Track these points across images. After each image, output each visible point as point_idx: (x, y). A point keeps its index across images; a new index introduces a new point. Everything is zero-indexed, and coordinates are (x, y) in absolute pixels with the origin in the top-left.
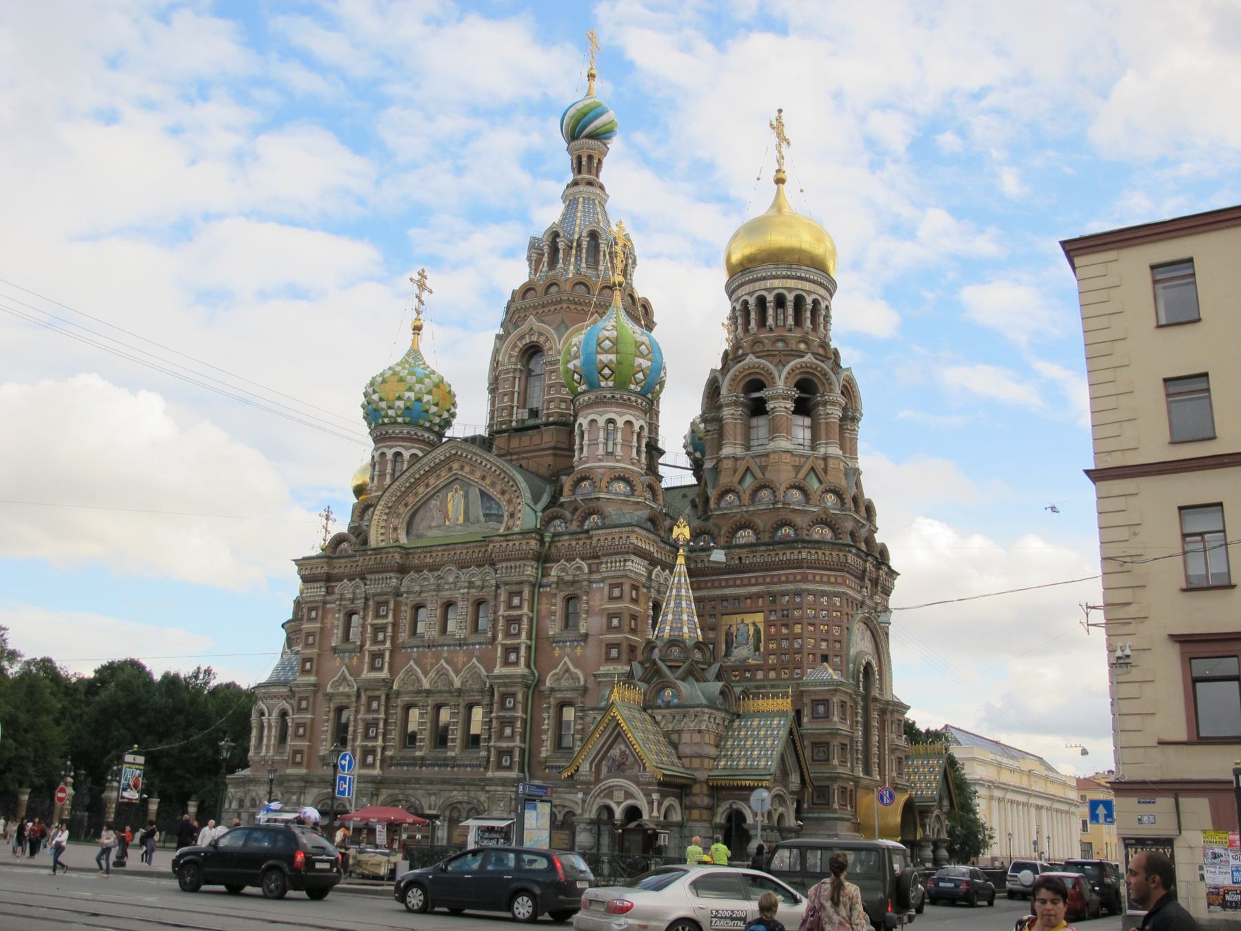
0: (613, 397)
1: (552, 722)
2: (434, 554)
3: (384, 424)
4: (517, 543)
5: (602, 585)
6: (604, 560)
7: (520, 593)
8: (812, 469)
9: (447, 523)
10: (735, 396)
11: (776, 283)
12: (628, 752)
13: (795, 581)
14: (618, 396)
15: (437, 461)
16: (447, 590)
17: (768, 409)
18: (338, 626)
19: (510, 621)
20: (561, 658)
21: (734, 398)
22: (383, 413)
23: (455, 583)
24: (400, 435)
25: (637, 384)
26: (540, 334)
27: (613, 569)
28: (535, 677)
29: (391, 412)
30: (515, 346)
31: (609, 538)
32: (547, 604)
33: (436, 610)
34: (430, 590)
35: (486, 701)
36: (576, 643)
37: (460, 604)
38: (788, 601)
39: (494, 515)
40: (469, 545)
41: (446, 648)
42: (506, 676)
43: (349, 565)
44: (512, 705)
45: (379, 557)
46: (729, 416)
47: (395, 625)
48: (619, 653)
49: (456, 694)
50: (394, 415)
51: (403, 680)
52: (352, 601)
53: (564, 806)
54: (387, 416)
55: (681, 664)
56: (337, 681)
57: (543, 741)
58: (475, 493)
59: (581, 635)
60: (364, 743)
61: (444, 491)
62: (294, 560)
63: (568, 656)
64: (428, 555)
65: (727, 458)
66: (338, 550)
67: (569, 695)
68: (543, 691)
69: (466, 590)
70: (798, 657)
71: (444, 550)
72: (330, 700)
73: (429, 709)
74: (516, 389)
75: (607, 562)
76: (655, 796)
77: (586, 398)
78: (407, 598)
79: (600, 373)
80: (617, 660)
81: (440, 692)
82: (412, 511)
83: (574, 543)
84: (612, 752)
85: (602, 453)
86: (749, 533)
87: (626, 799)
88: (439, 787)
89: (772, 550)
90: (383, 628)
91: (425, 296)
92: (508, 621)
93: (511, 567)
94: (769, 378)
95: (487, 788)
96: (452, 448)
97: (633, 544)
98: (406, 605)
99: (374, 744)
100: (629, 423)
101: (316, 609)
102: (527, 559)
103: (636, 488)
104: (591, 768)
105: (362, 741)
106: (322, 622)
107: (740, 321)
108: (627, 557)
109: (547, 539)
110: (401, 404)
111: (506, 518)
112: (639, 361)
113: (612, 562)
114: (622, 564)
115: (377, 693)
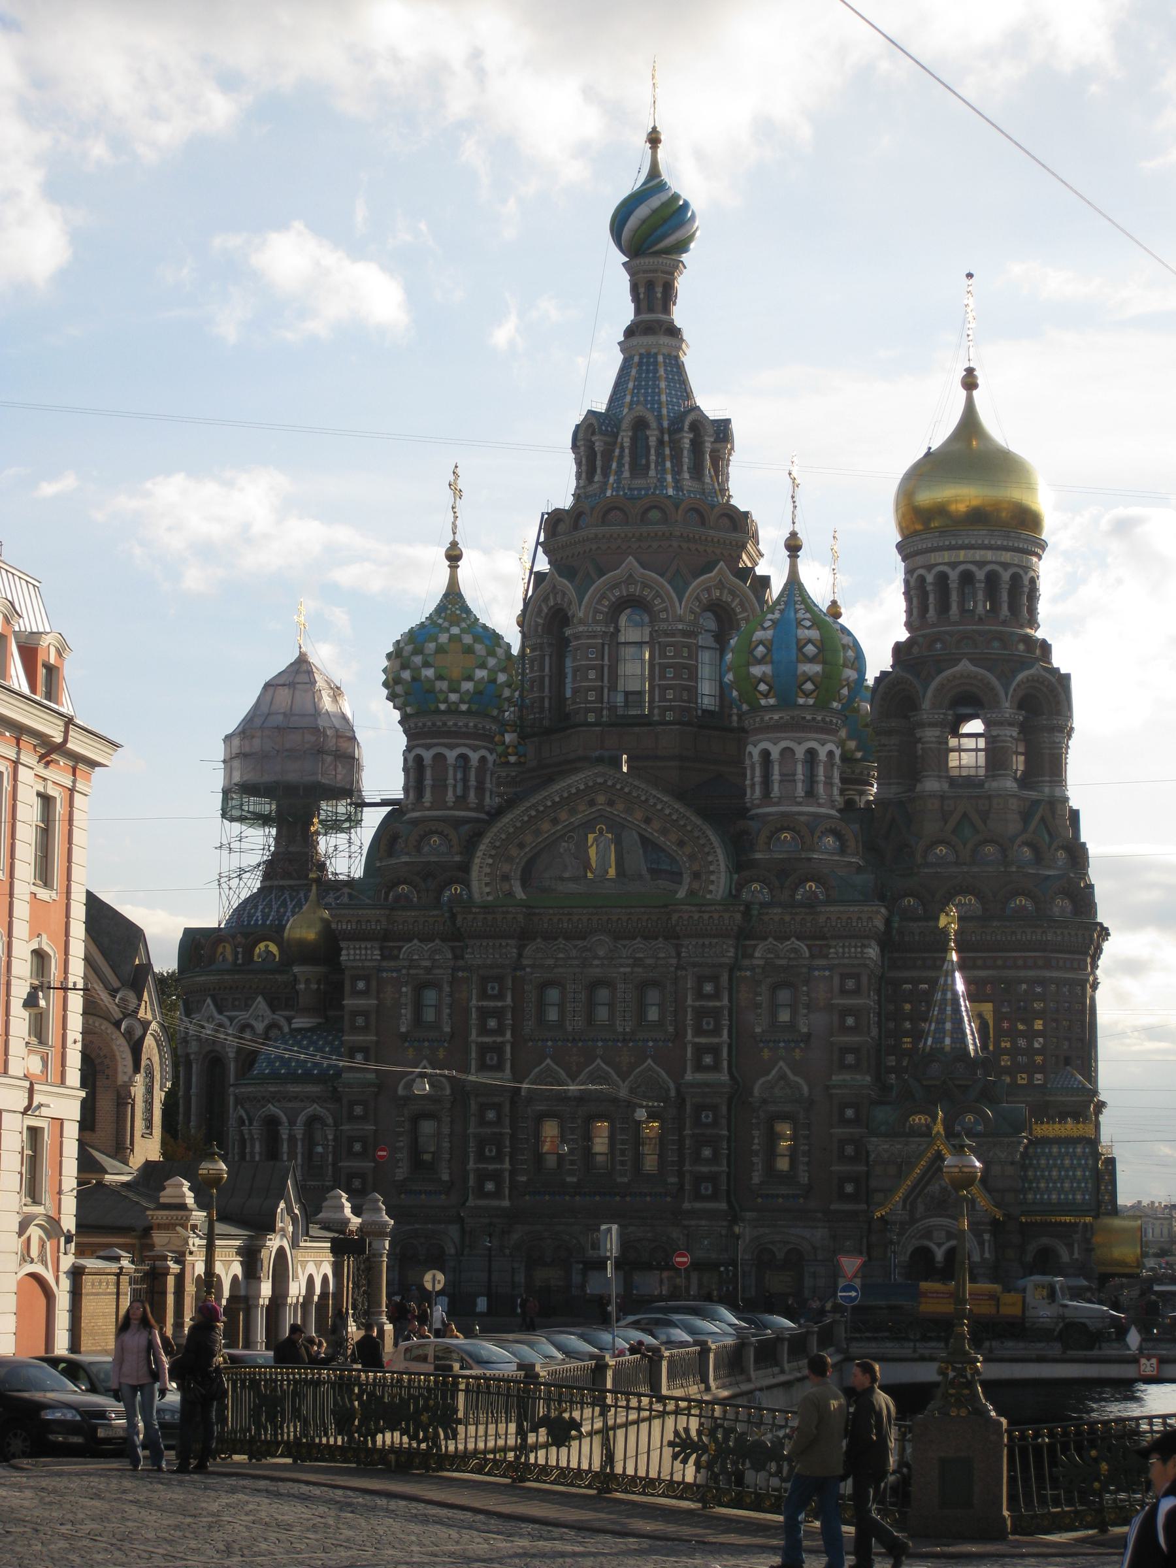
0: (814, 719)
3: (437, 711)
5: (827, 973)
6: (833, 943)
7: (715, 979)
8: (1043, 819)
9: (590, 875)
11: (989, 555)
19: (700, 1014)
21: (942, 716)
24: (464, 729)
25: (840, 701)
26: (645, 585)
27: (847, 955)
29: (453, 697)
30: (603, 597)
36: (793, 1045)
38: (1025, 990)
40: (633, 910)
41: (600, 1044)
46: (934, 739)
52: (428, 970)
54: (446, 701)
55: (970, 1083)
69: (628, 970)
70: (1039, 1059)
73: (579, 1121)
74: (606, 662)
75: (835, 947)
76: (987, 1237)
77: (776, 717)
79: (800, 687)
85: (803, 794)
86: (970, 900)
87: (948, 1240)
90: (498, 1014)
93: (704, 944)
95: (686, 1223)
99: (499, 1167)
101: (367, 978)
104: (904, 1208)
106: (378, 998)
107: (931, 599)
108: (866, 942)
111: (687, 879)
113: (843, 946)
114: (859, 950)
115: (496, 1100)
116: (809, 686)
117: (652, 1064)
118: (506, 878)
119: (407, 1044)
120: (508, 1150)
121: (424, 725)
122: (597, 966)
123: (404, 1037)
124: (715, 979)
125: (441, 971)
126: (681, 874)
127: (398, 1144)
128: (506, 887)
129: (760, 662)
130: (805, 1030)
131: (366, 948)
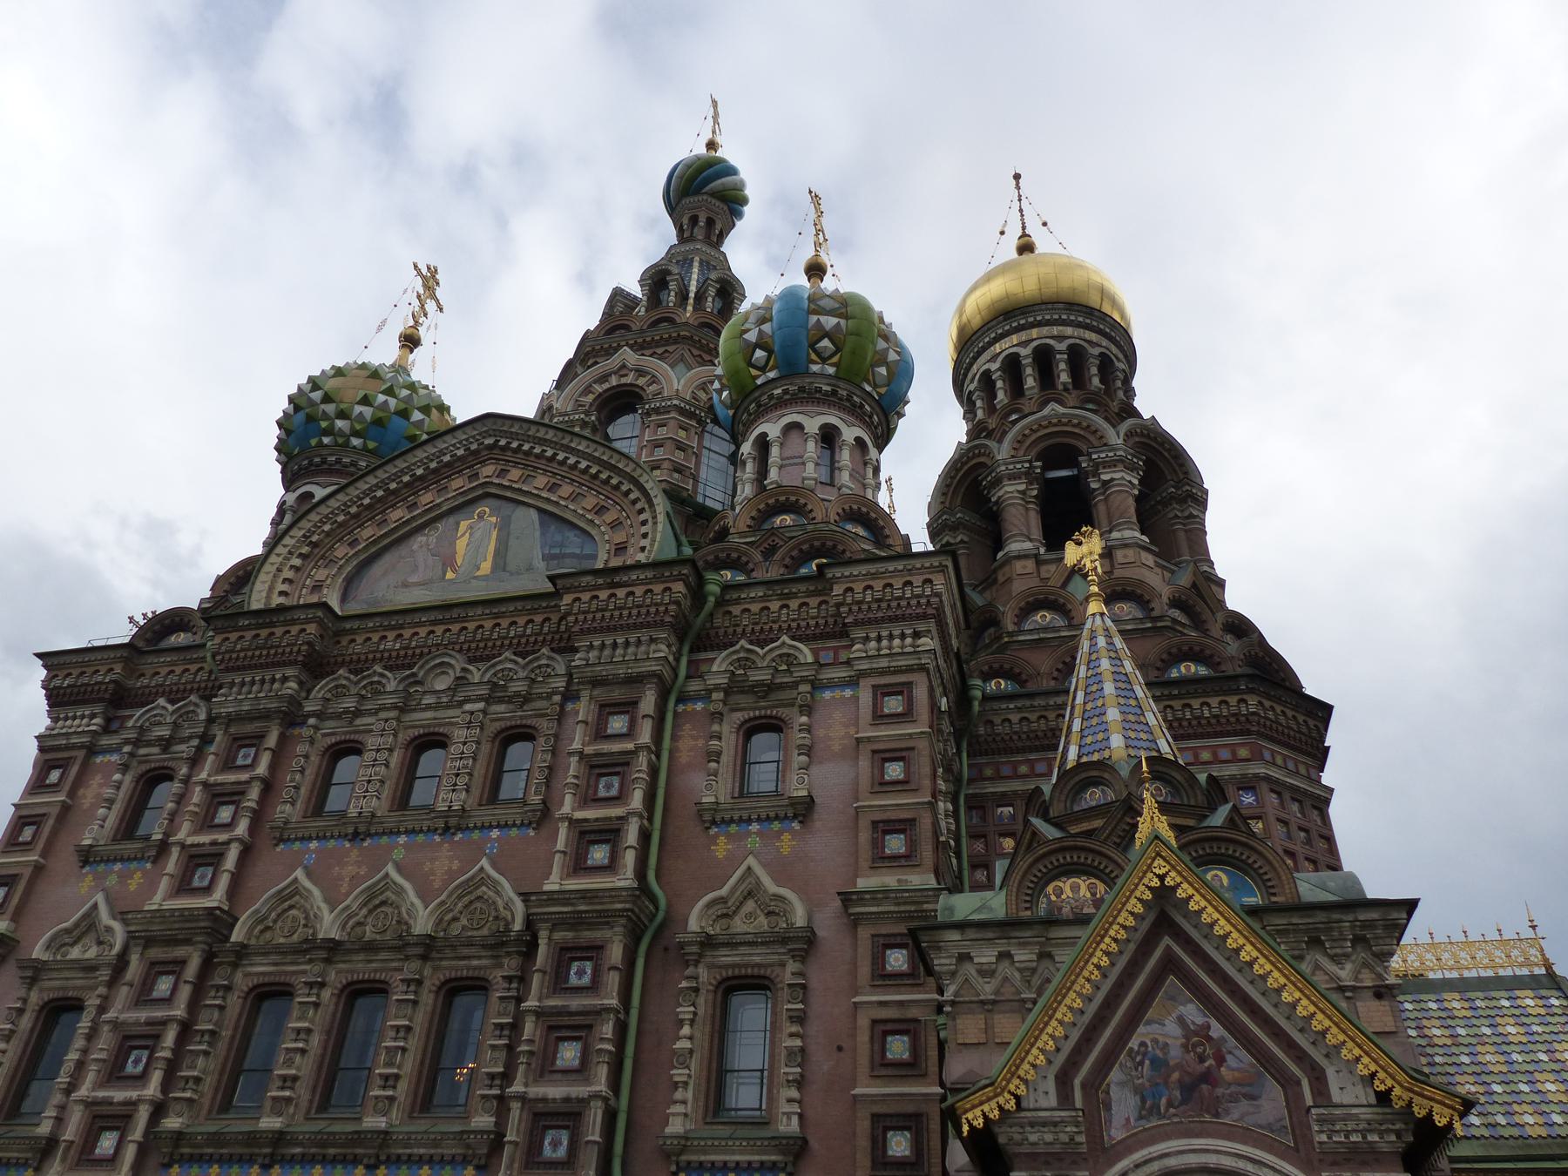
0: (834, 393)
1: (703, 1032)
2: (407, 633)
3: (320, 444)
4: (639, 591)
5: (848, 693)
6: (859, 633)
7: (628, 707)
8: (1194, 585)
9: (450, 575)
10: (1030, 462)
11: (1069, 331)
12: (1217, 1030)
13: (1235, 760)
14: (845, 393)
15: (447, 458)
16: (429, 707)
17: (1094, 485)
18: (111, 801)
19: (598, 767)
20: (733, 861)
21: (1027, 465)
22: (324, 424)
23: (453, 690)
25: (875, 386)
26: (641, 372)
28: (657, 909)
29: (339, 423)
30: (587, 390)
31: (878, 585)
32: (695, 738)
33: (391, 750)
34: (383, 708)
35: (510, 965)
36: (776, 826)
37: (459, 734)
41: (402, 839)
42: (584, 895)
43: (178, 670)
44: (586, 980)
45: (264, 633)
47: (268, 786)
48: (912, 844)
49: (419, 950)
50: (347, 431)
51: (264, 918)
52: (166, 744)
56: (67, 931)
57: (676, 1085)
59: (794, 802)
60: (101, 1094)
61: (451, 520)
62: (39, 656)
63: (755, 857)
64: (391, 635)
65: (1022, 556)
66: (164, 644)
67: (757, 956)
68: (681, 945)
69: (481, 705)
71: (435, 623)
72: (32, 982)
73: (326, 994)
75: (867, 639)
77: (778, 391)
78: (316, 728)
79: (812, 346)
80: (906, 860)
81: (370, 948)
83: (775, 606)
84: (1143, 1033)
89: (1171, 697)
90: (233, 795)
91: (431, 306)
92: (592, 767)
94: (1092, 438)
96: (487, 434)
97: (938, 595)
98: (312, 742)
100: (859, 441)
101: (63, 765)
102: (660, 624)
103: (890, 541)
105: (99, 1085)
106: (72, 793)
107: (999, 384)
108: (921, 627)
109: (713, 588)
110: (367, 412)
112: (882, 344)
113: (879, 639)
114: (909, 641)
116: (826, 343)
117: (488, 868)
119: (87, 868)
121: (300, 469)
122: (429, 707)
123: (87, 857)
124: (628, 707)
125: (183, 747)
126: (595, 557)
128: (314, 599)
130: (805, 793)
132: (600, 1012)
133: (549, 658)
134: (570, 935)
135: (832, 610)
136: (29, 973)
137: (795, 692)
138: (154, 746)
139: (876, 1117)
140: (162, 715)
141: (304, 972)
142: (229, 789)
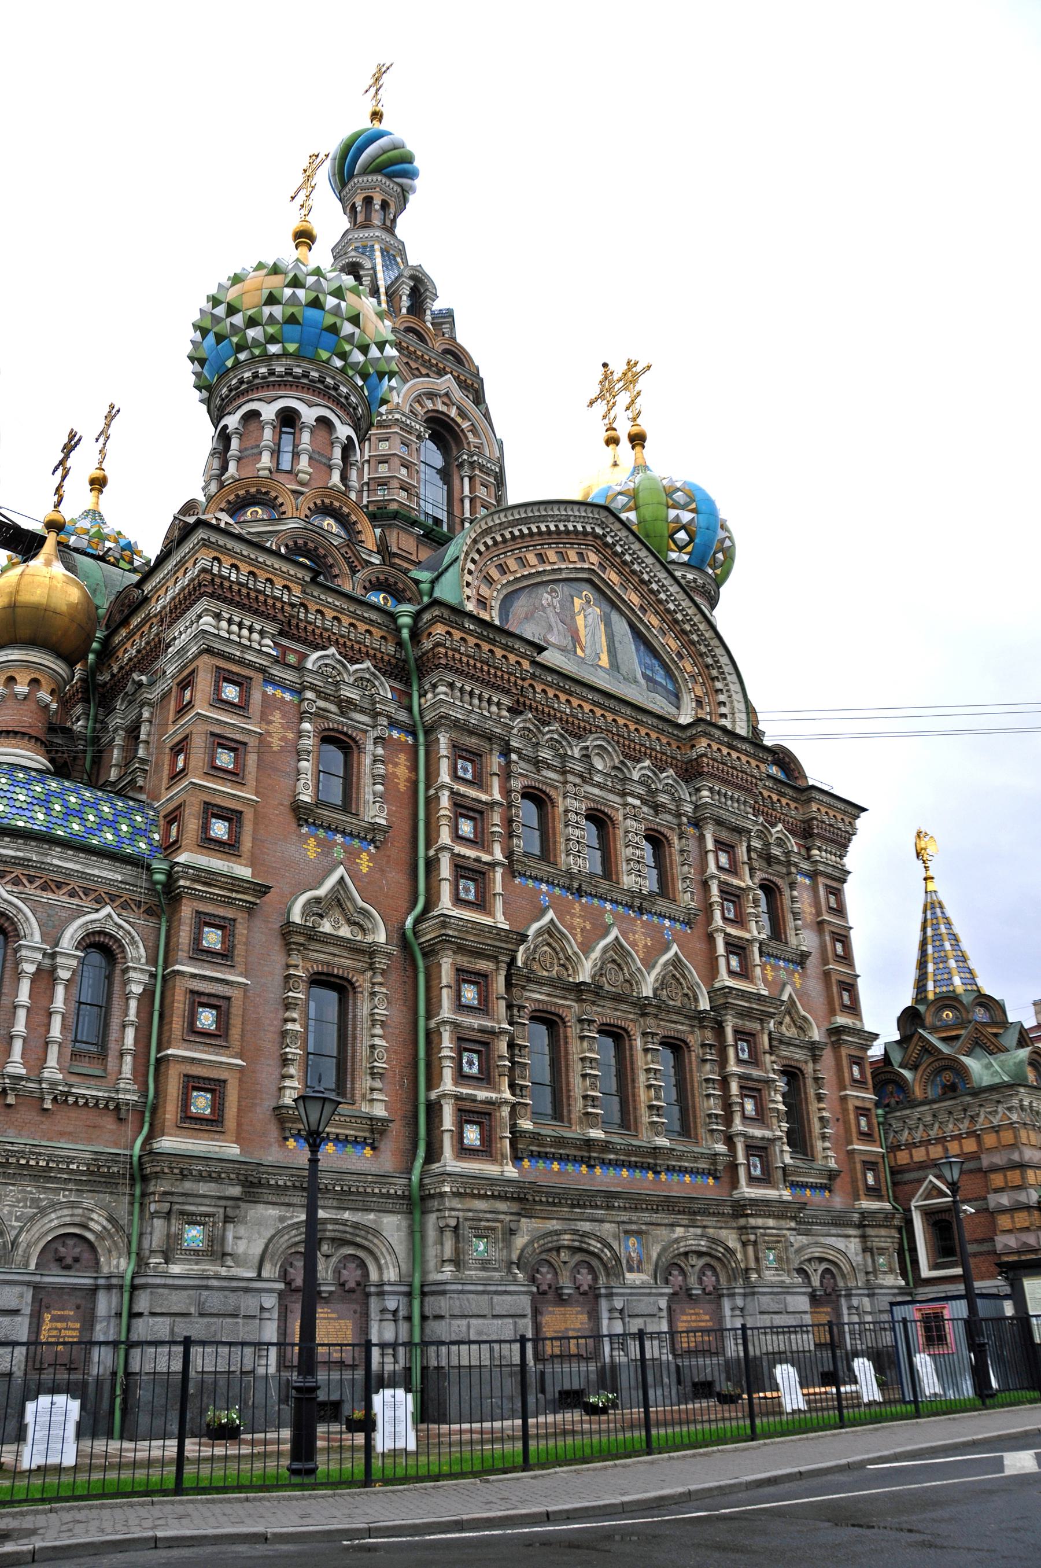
2: (575, 702)
4: (744, 759)
5: (807, 881)
9: (579, 652)
16: (598, 785)
26: (462, 413)
29: (358, 357)
30: (418, 400)
36: (791, 966)
39: (660, 684)
43: (346, 621)
45: (486, 647)
52: (345, 706)
53: (821, 1260)
56: (318, 900)
58: (621, 626)
60: (465, 1091)
64: (563, 697)
69: (637, 802)
82: (510, 589)
88: (646, 1216)
95: (752, 1221)
99: (493, 1096)
115: (484, 965)
118: (482, 602)
119: (305, 830)
120: (507, 1063)
123: (301, 814)
127: (290, 1026)
129: (683, 507)
131: (251, 629)
132: (769, 1082)
133: (675, 780)
134: (740, 1022)
135: (800, 817)
136: (301, 939)
137: (784, 870)
138: (331, 702)
139: (864, 1162)
140: (334, 668)
141: (570, 1007)
142: (469, 803)
